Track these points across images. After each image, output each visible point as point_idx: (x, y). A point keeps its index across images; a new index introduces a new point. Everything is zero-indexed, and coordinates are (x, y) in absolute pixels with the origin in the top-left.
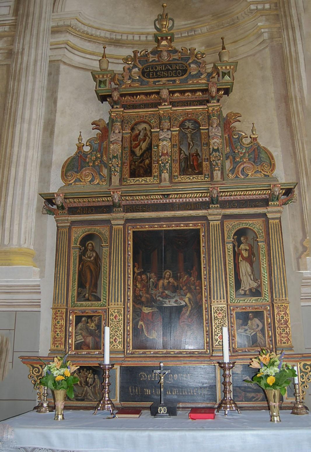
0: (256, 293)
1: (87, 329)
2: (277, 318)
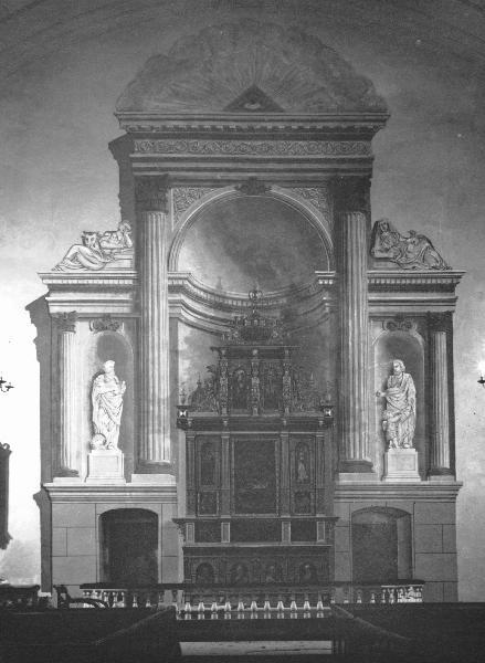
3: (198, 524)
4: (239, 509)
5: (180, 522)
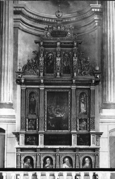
1: (32, 123)
2: (91, 121)
3: (27, 136)
4: (49, 128)
5: (17, 135)
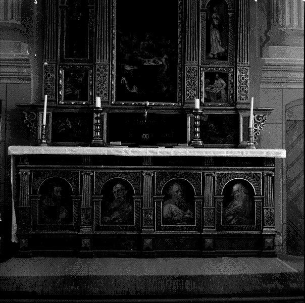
0: (222, 57)
2: (239, 78)
